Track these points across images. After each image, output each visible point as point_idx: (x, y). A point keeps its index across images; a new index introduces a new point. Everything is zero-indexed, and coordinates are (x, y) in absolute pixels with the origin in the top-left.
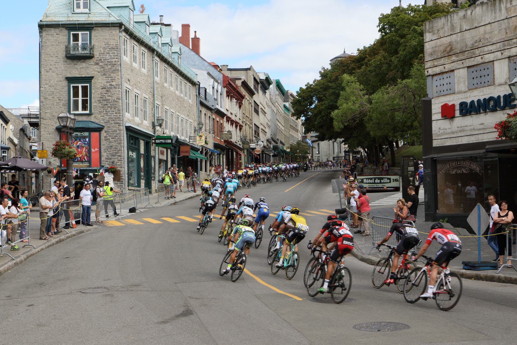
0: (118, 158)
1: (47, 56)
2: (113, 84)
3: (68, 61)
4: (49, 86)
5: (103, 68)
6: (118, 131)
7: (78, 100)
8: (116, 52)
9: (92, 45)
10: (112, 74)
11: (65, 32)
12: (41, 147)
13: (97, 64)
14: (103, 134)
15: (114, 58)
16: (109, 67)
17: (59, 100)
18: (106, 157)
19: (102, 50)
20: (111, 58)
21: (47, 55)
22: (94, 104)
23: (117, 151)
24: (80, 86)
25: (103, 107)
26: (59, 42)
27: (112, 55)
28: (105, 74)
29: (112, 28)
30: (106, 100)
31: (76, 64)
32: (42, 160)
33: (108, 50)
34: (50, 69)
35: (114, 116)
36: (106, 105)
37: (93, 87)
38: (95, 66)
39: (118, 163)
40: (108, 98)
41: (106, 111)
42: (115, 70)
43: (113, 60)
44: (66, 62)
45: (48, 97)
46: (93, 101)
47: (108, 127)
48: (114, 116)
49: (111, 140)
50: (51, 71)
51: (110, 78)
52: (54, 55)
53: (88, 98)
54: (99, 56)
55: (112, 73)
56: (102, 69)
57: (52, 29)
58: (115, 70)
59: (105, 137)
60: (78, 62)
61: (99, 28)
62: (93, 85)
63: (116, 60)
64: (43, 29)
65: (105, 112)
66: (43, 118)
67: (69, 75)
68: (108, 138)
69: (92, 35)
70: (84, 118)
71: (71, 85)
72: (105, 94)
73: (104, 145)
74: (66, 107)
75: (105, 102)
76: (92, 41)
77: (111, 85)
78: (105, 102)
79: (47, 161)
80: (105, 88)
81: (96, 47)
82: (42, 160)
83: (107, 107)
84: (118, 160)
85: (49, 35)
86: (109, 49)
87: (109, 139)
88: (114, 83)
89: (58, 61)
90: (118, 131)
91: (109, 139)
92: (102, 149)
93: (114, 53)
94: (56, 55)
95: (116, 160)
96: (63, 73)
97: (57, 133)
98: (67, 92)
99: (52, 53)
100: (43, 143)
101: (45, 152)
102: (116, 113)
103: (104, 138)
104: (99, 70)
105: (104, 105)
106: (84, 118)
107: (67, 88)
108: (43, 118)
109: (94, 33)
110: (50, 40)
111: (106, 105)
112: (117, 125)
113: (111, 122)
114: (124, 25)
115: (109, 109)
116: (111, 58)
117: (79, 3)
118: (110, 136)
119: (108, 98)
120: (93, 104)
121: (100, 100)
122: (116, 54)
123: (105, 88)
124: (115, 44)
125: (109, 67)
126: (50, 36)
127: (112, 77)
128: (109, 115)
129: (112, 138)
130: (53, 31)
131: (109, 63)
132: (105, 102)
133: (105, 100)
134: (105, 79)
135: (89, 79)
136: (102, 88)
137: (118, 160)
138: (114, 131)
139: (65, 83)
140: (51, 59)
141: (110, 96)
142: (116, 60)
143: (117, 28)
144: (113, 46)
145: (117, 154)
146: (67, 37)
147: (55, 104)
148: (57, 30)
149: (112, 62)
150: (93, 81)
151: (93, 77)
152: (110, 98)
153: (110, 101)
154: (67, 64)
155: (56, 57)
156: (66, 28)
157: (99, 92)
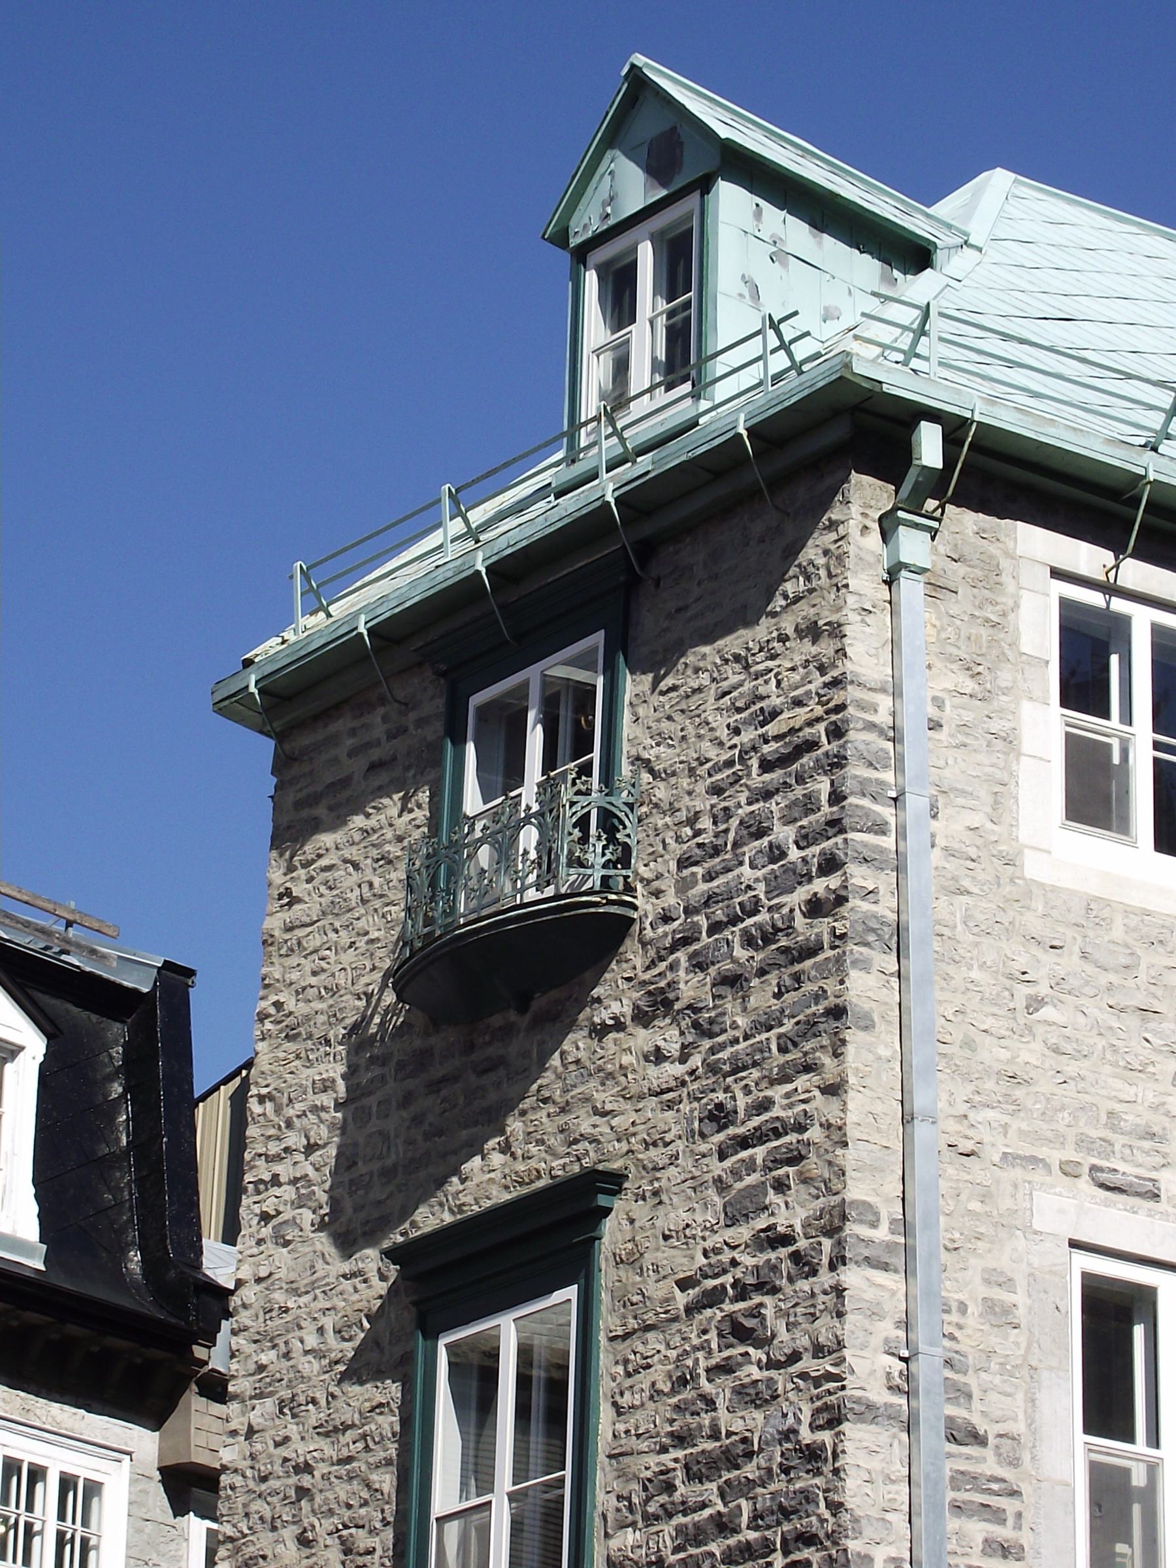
10: (777, 1093)
19: (703, 803)
20: (776, 886)
28: (720, 1116)
33: (757, 779)
36: (724, 1525)
38: (643, 1039)
42: (810, 1028)
51: (759, 1153)
53: (568, 1473)
54: (683, 886)
58: (810, 1028)
72: (715, 1371)
77: (774, 1239)
80: (713, 1298)
86: (766, 766)
114: (934, 415)
125: (761, 997)
134: (718, 1168)
142: (819, 886)
144: (802, 713)
152: (755, 1422)
153: (750, 1470)
154: (434, 1086)
157: (659, 1375)
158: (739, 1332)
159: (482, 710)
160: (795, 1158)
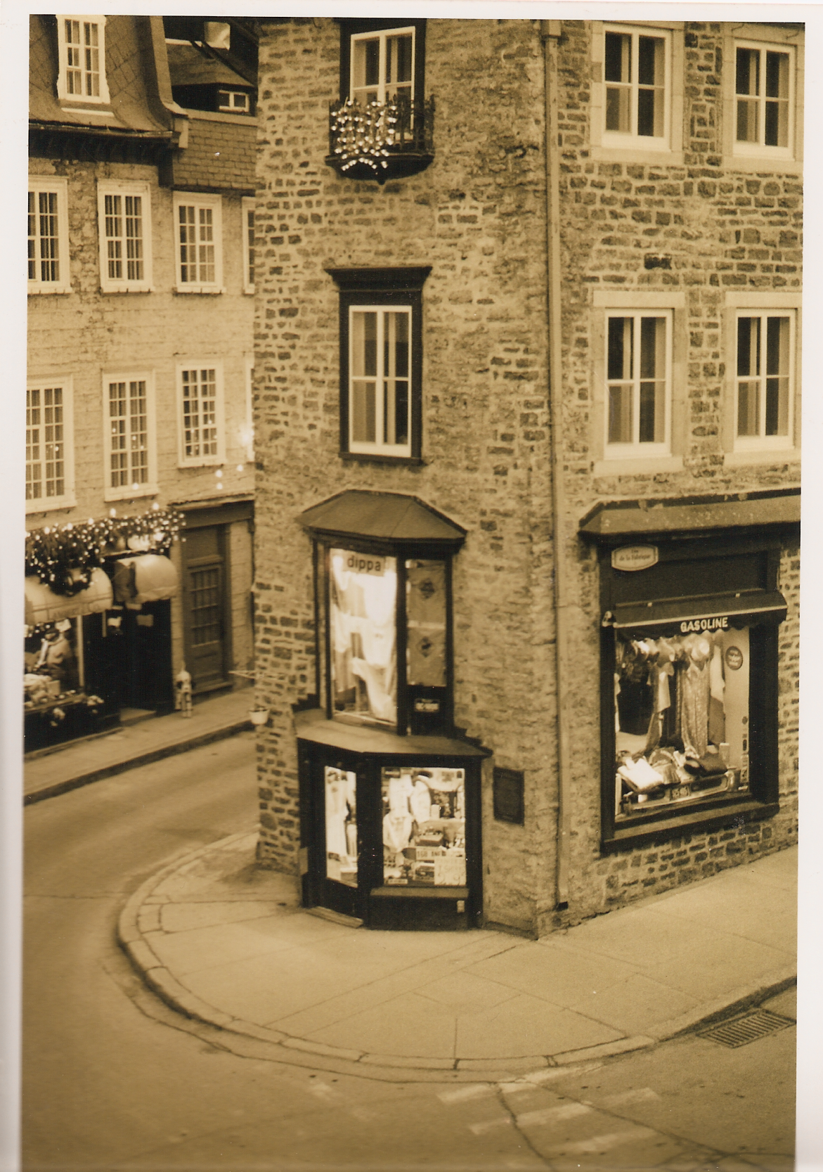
24: (380, 310)
26: (312, 93)
67: (342, 262)
70: (396, 482)
74: (336, 417)
76: (428, 76)
81: (443, 109)
89: (308, 187)
96: (326, 247)
97: (305, 541)
98: (336, 343)
106: (396, 482)
110: (282, 80)
126: (282, 61)
139: (328, 295)
151: (425, 271)
155: (304, 164)
159: (358, 43)
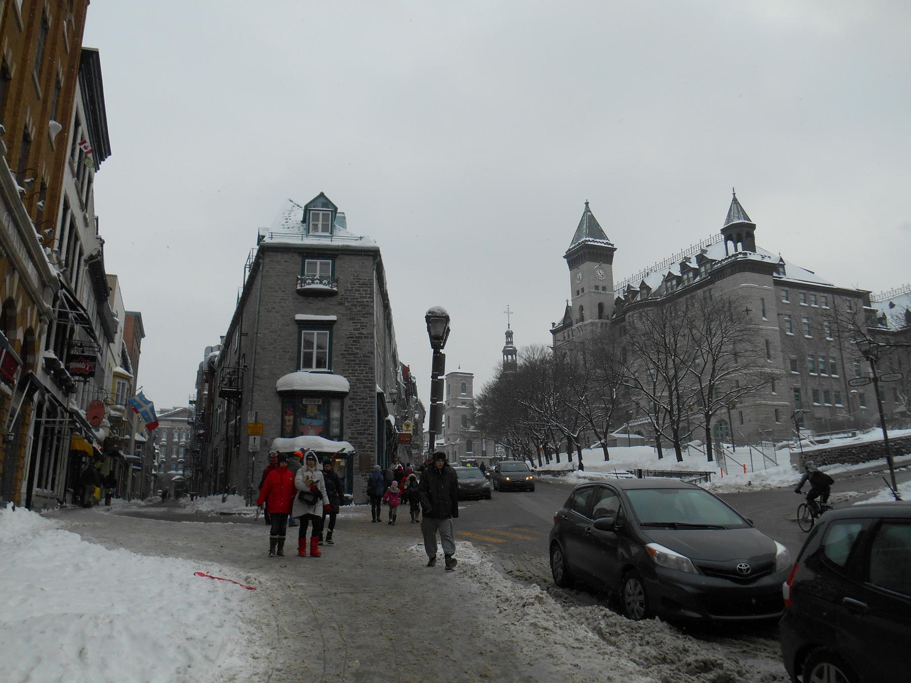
0: (367, 438)
1: (270, 290)
2: (363, 332)
3: (300, 297)
4: (270, 332)
5: (350, 309)
6: (369, 399)
7: (311, 354)
8: (369, 289)
9: (336, 278)
10: (362, 319)
11: (298, 259)
12: (254, 419)
13: (341, 304)
14: (348, 402)
15: (366, 298)
16: (359, 308)
17: (284, 351)
18: (350, 436)
20: (360, 297)
21: (270, 288)
22: (336, 359)
23: (366, 427)
25: (348, 364)
26: (288, 273)
27: (364, 293)
28: (351, 319)
29: (365, 257)
30: (354, 354)
31: (312, 303)
32: (255, 438)
34: (272, 308)
35: (363, 376)
36: (353, 361)
37: (334, 336)
38: (338, 307)
39: (367, 445)
40: (356, 351)
41: (352, 370)
42: (367, 314)
43: (365, 300)
44: (297, 299)
45: (267, 346)
46: (334, 354)
47: (355, 392)
48: (363, 376)
49: (358, 410)
50: (274, 310)
51: (359, 324)
52: (280, 289)
55: (363, 317)
56: (348, 312)
57: (279, 254)
58: (367, 314)
59: (349, 407)
60: (314, 300)
61: (346, 257)
62: (334, 332)
63: (369, 300)
64: (266, 253)
65: (350, 371)
66: (258, 377)
68: (354, 408)
69: (336, 265)
71: (303, 331)
73: (347, 417)
75: (352, 356)
76: (336, 274)
77: (361, 334)
78: (352, 358)
79: (261, 439)
80: (352, 337)
82: (255, 438)
83: (354, 364)
84: (368, 441)
85: (274, 262)
86: (359, 284)
87: (356, 410)
88: (365, 332)
90: (369, 399)
91: (356, 410)
92: (345, 424)
93: (366, 290)
94: (283, 289)
95: (365, 441)
99: (277, 287)
100: (256, 412)
101: (258, 425)
102: (366, 373)
103: (348, 409)
104: (343, 312)
105: (350, 361)
107: (296, 335)
108: (258, 377)
109: (338, 262)
111: (353, 361)
112: (368, 389)
113: (358, 385)
115: (357, 367)
116: (360, 297)
117: (317, 225)
118: (357, 405)
119: (356, 351)
120: (334, 359)
121: (344, 354)
122: (369, 292)
123: (350, 337)
124: (367, 278)
125: (359, 308)
127: (363, 323)
128: (357, 374)
129: (359, 409)
130: (279, 257)
131: (358, 304)
132: (352, 358)
133: (351, 354)
135: (328, 325)
136: (347, 338)
137: (368, 441)
138: (362, 399)
139: (294, 328)
140: (275, 294)
141: (356, 348)
142: (369, 300)
143: (371, 258)
145: (367, 432)
146: (300, 267)
147: (278, 357)
148: (286, 257)
149: (363, 302)
150: (335, 327)
152: (358, 351)
153: (359, 356)
155: (283, 291)
156: (300, 253)
158: (354, 341)
160: (366, 326)
